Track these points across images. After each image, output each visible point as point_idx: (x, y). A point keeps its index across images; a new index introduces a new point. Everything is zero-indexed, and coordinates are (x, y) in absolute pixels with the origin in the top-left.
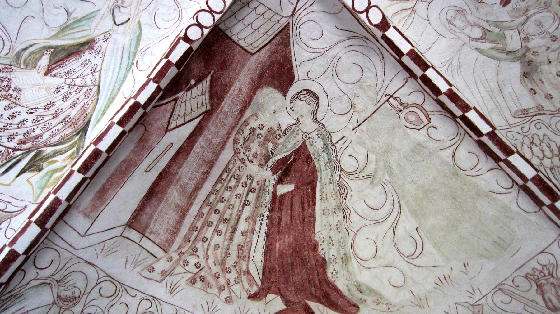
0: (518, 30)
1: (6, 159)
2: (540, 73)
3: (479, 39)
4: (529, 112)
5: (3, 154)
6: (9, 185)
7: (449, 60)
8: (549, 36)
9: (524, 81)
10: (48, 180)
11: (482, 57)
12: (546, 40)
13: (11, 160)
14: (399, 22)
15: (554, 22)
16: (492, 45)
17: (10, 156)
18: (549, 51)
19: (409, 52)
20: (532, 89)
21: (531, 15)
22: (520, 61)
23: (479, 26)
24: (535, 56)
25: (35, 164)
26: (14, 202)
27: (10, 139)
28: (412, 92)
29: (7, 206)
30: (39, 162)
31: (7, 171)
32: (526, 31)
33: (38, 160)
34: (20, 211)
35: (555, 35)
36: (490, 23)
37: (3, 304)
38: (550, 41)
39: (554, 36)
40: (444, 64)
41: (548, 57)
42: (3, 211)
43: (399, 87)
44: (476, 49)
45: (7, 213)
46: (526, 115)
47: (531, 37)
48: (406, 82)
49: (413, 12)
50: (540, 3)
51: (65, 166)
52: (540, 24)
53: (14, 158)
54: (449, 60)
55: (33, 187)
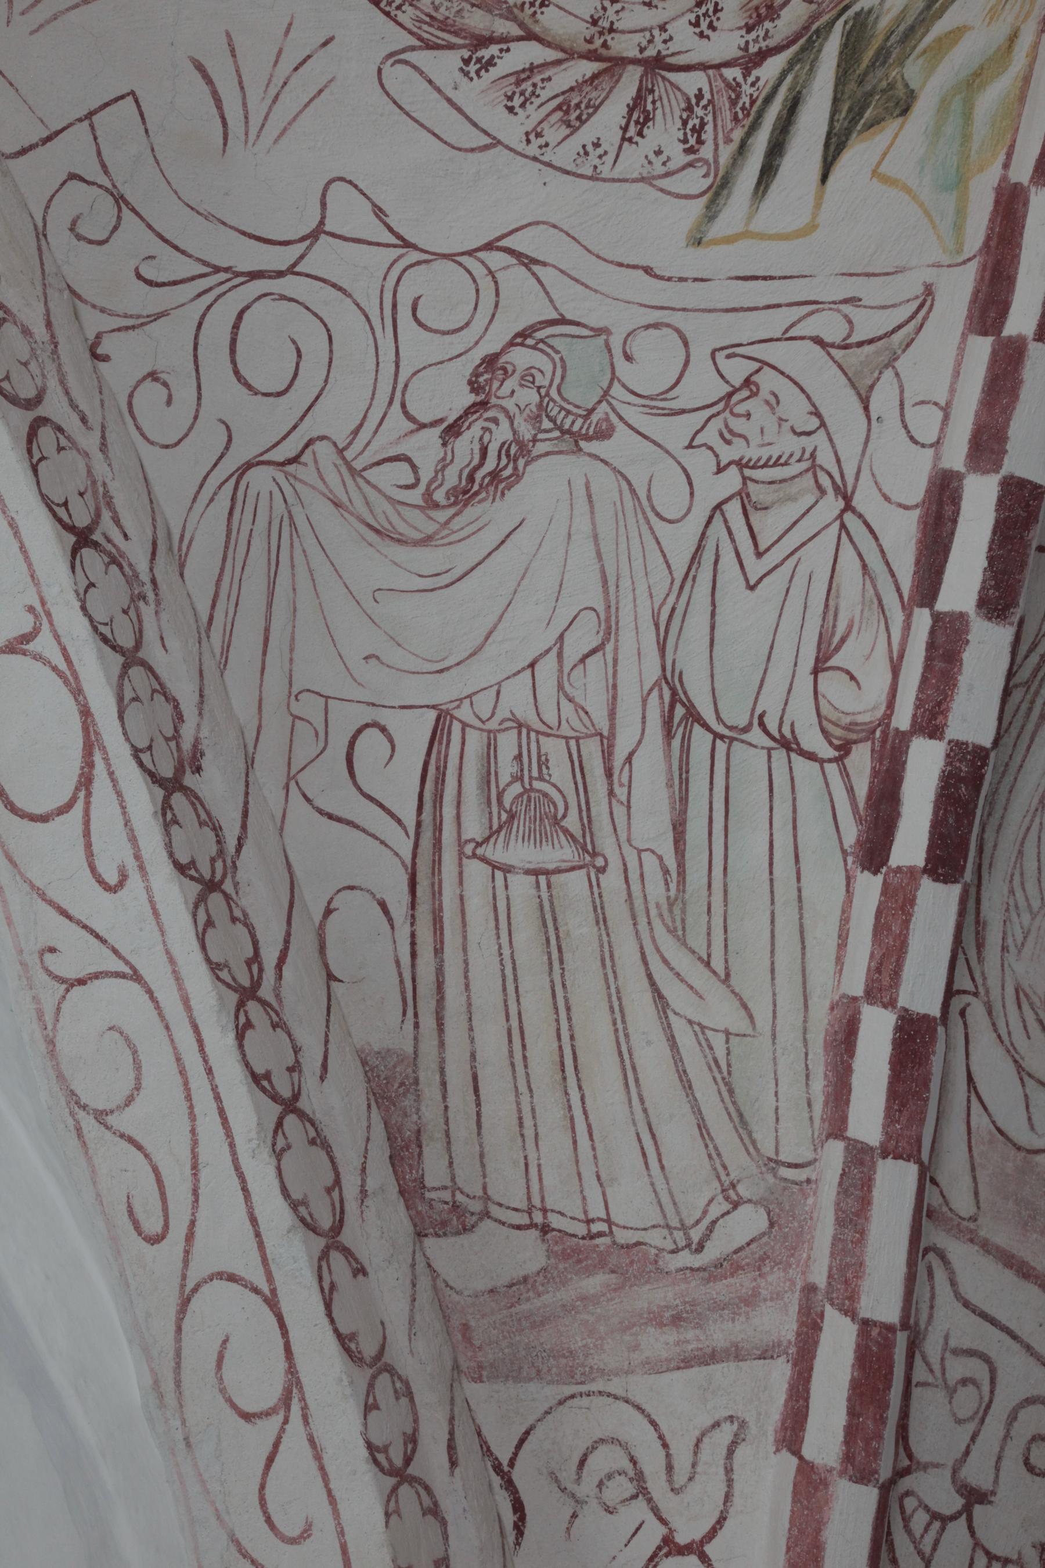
1: (736, 119)
5: (710, 102)
6: (811, 228)
10: (966, 138)
13: (760, 114)
17: (747, 100)
25: (868, 87)
26: (870, 291)
27: (704, 25)
29: (850, 322)
30: (880, 73)
31: (768, 171)
33: (872, 65)
34: (912, 317)
37: (1029, 697)
42: (846, 347)
45: (867, 349)
51: (1013, 38)
53: (768, 100)
55: (915, 198)
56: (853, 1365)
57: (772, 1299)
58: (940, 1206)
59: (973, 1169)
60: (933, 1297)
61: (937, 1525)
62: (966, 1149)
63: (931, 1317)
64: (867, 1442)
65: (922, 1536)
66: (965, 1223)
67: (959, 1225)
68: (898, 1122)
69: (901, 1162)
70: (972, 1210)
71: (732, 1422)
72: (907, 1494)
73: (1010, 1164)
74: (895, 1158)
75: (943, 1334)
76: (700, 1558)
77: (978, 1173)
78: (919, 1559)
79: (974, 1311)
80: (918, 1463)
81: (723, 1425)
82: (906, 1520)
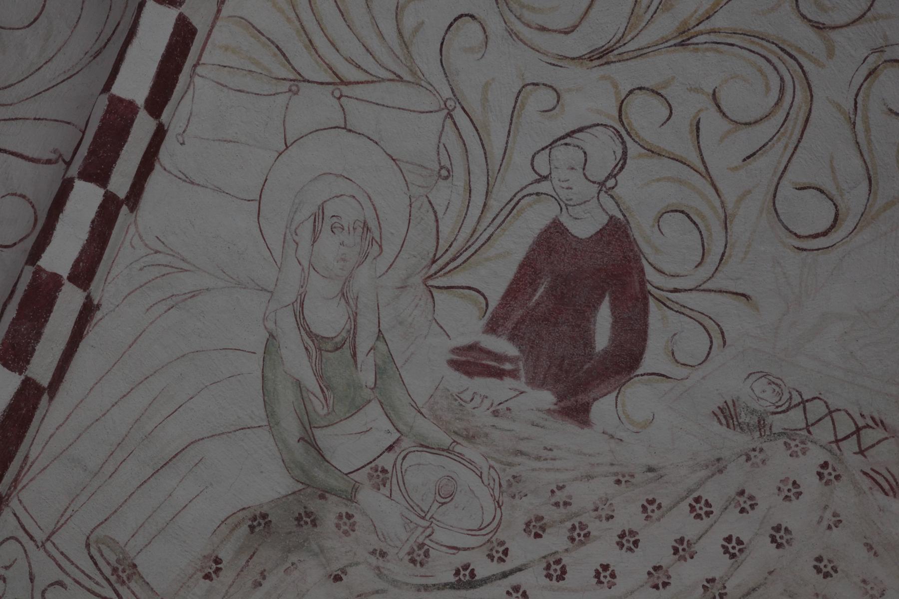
0: (398, 440)
2: (288, 565)
3: (310, 334)
4: (132, 585)
7: (183, 260)
8: (420, 540)
9: (237, 526)
11: (253, 366)
12: (404, 537)
14: (227, 48)
15: (471, 532)
16: (311, 383)
18: (373, 560)
19: (121, 100)
20: (218, 561)
21: (460, 455)
22: (300, 486)
23: (354, 317)
24: (338, 526)
28: (24, 197)
32: (406, 464)
35: (431, 552)
36: (381, 346)
38: (407, 549)
39: (427, 554)
40: (160, 247)
41: (350, 565)
43: (26, 153)
44: (272, 336)
46: (113, 579)
47: (395, 488)
48: (49, 162)
49: (288, 84)
50: (510, 465)
52: (445, 497)
54: (183, 260)
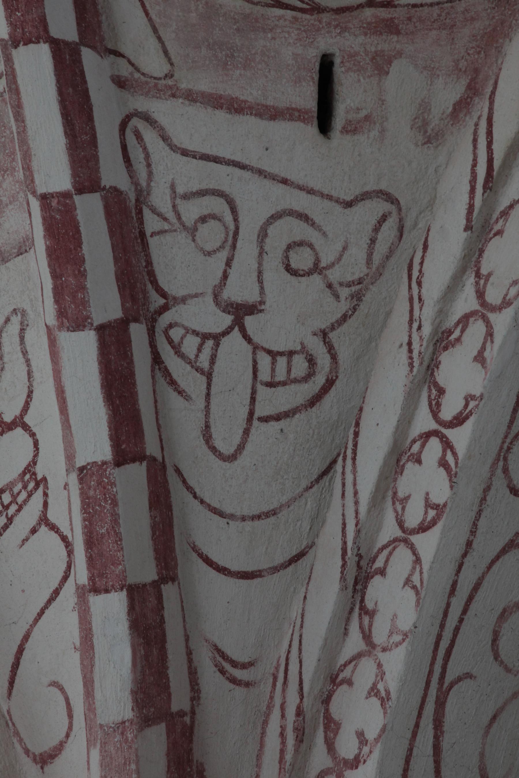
56: (45, 236)
57: (11, 203)
58: (131, 74)
59: (155, 30)
60: (147, 156)
61: (210, 343)
62: (143, 14)
63: (150, 174)
64: (74, 297)
65: (197, 356)
66: (163, 82)
67: (156, 85)
68: (17, 10)
69: (31, 46)
70: (166, 68)
71: (16, 314)
72: (171, 326)
73: (194, 15)
74: (25, 44)
75: (168, 185)
76: (23, 428)
77: (161, 33)
78: (198, 375)
79: (194, 157)
80: (175, 298)
81: (12, 318)
82: (177, 349)
